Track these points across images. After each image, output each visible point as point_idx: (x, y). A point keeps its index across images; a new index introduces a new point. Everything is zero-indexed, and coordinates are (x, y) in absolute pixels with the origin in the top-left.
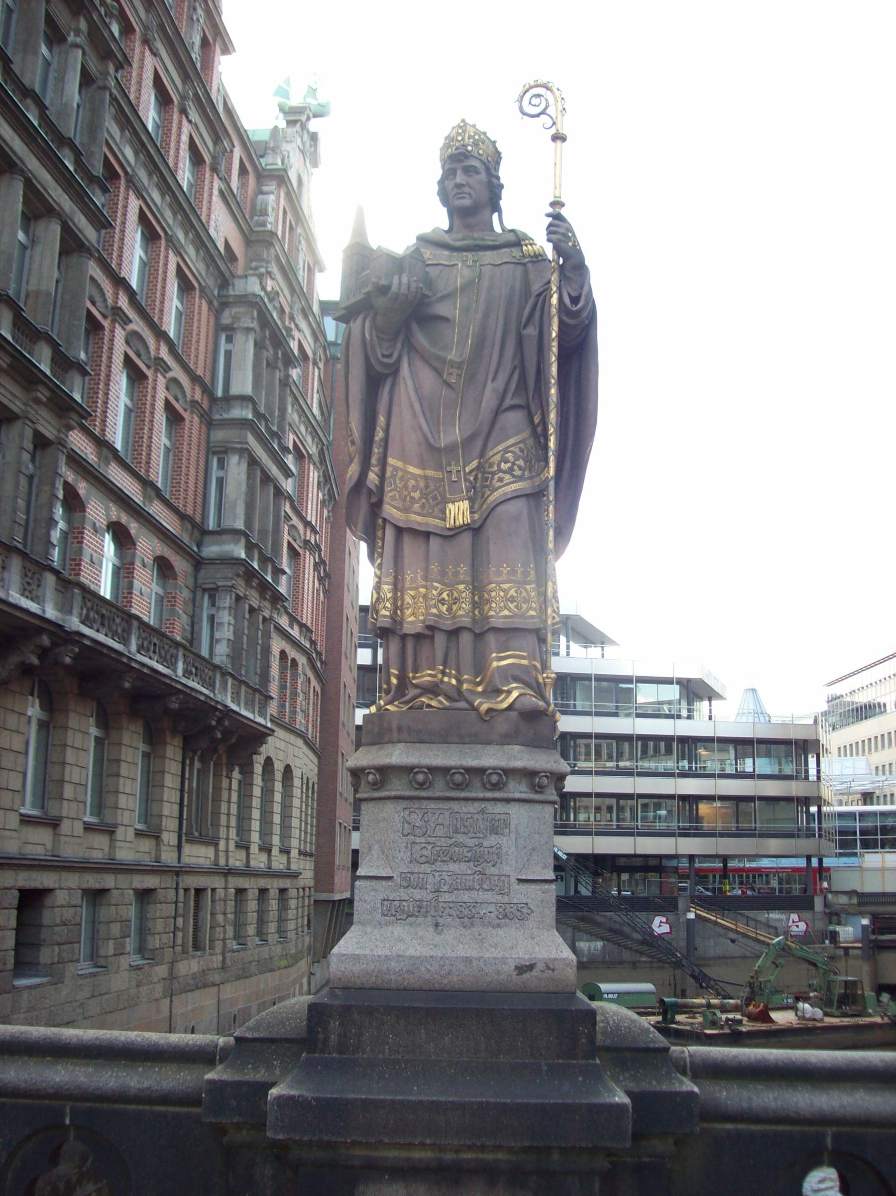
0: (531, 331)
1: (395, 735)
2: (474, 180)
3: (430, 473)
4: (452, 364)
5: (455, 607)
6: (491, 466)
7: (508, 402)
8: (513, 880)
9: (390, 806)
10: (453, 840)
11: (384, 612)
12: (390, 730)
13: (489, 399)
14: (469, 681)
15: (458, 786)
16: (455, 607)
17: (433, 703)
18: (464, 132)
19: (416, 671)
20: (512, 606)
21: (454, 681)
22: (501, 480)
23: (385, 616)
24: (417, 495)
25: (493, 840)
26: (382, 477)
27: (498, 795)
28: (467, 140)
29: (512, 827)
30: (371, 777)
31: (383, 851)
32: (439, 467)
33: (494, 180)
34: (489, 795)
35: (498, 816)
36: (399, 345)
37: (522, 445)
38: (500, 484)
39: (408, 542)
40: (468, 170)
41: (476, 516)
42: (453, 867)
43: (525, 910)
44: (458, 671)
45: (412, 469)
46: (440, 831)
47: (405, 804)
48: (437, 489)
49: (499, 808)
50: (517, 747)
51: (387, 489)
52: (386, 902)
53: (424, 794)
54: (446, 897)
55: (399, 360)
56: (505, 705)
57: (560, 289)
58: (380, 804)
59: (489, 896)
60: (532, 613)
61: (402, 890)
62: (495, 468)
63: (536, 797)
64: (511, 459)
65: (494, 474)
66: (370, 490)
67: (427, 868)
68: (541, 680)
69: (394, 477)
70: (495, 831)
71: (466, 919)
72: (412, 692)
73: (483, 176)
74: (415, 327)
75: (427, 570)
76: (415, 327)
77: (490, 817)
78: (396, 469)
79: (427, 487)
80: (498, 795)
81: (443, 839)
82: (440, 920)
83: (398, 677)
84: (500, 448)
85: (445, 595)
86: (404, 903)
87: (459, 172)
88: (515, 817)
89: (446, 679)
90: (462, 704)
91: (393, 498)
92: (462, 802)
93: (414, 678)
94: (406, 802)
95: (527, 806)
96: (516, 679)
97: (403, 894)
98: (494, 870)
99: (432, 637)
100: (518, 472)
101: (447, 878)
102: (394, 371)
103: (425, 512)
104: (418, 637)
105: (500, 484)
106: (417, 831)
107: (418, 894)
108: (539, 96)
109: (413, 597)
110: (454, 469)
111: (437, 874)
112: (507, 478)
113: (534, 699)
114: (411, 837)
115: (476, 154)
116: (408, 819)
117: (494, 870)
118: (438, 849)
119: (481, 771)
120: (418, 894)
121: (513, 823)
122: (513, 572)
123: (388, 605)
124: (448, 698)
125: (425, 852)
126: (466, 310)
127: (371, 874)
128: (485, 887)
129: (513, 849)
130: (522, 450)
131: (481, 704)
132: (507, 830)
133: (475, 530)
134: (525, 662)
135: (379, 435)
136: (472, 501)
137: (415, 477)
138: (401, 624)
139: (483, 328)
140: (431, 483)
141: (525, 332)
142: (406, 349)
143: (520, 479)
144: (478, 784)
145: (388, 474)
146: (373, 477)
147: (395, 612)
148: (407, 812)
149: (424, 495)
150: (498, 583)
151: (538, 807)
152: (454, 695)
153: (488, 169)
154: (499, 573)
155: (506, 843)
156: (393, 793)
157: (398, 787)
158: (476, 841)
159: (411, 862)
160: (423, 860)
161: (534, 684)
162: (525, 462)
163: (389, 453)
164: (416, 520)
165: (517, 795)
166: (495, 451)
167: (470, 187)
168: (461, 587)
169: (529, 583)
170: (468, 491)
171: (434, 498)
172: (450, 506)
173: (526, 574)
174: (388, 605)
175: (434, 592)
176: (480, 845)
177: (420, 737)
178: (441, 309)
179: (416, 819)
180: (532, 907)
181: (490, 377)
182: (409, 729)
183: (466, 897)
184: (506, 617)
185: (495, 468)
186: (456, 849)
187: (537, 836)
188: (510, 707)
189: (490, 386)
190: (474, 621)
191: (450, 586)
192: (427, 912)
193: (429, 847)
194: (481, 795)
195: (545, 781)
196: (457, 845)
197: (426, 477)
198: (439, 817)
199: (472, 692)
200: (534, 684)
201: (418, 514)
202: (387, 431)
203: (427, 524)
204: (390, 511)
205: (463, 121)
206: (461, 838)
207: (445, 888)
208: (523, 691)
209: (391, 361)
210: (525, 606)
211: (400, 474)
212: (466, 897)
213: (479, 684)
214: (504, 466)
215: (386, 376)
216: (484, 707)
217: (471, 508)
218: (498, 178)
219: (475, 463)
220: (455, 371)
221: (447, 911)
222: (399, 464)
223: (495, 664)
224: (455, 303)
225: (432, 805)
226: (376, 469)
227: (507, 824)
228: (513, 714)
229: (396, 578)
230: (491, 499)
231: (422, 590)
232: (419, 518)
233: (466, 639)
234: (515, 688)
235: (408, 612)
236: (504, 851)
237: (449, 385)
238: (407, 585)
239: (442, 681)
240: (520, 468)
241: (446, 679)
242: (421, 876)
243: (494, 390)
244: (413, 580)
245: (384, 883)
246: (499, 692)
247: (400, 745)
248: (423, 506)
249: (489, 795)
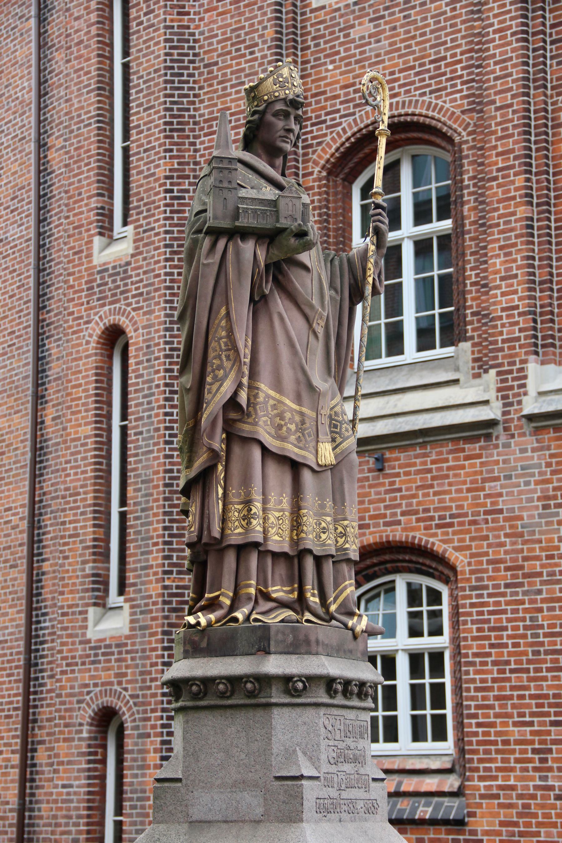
1: (314, 648)
9: (310, 712)
16: (324, 536)
24: (293, 427)
45: (288, 402)
58: (298, 710)
69: (266, 403)
78: (268, 396)
103: (301, 445)
109: (278, 518)
137: (292, 410)
140: (307, 420)
156: (309, 700)
164: (292, 450)
197: (302, 414)
203: (304, 457)
232: (296, 450)
248: (299, 439)
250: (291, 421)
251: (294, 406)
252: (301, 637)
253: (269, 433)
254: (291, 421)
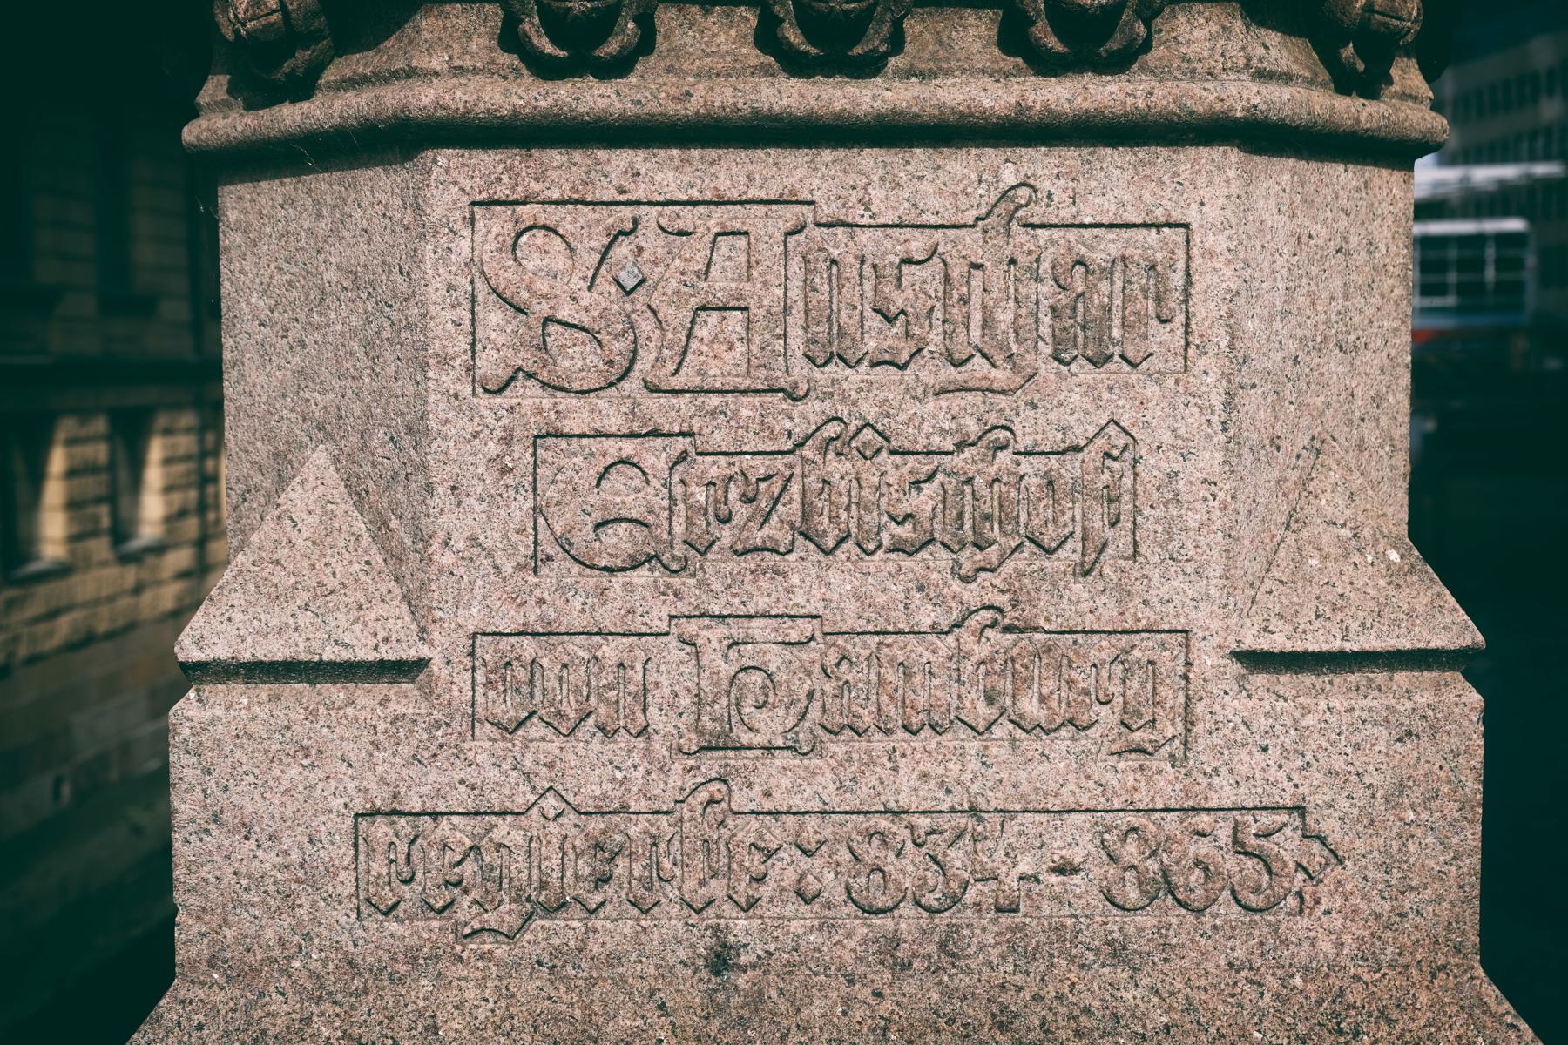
8: (1207, 660)
10: (814, 409)
25: (1072, 402)
29: (1206, 311)
31: (358, 495)
35: (1111, 245)
42: (824, 586)
43: (1288, 846)
46: (721, 354)
49: (1114, 183)
52: (380, 830)
53: (593, 97)
54: (782, 781)
59: (1054, 767)
61: (483, 745)
70: (1085, 339)
71: (908, 919)
77: (1052, 247)
81: (747, 408)
82: (740, 926)
86: (503, 830)
88: (1219, 242)
92: (869, 159)
94: (488, 160)
95: (1281, 176)
97: (488, 766)
98: (1081, 602)
101: (775, 659)
107: (593, 768)
111: (713, 636)
114: (528, 395)
116: (505, 275)
117: (1081, 602)
118: (715, 468)
120: (593, 768)
121: (1215, 279)
125: (624, 493)
127: (277, 651)
128: (1030, 706)
129: (1209, 460)
132: (1165, 337)
148: (497, 225)
155: (1169, 419)
158: (969, 413)
159: (537, 561)
160: (619, 540)
165: (1241, 96)
176: (994, 439)
180: (1330, 826)
183: (911, 776)
186: (836, 467)
187: (1334, 365)
192: (656, 878)
193: (655, 457)
206: (867, 393)
207: (770, 725)
212: (911, 776)
221: (785, 870)
225: (663, 172)
227: (1168, 295)
236: (1154, 466)
242: (610, 651)
245: (366, 696)
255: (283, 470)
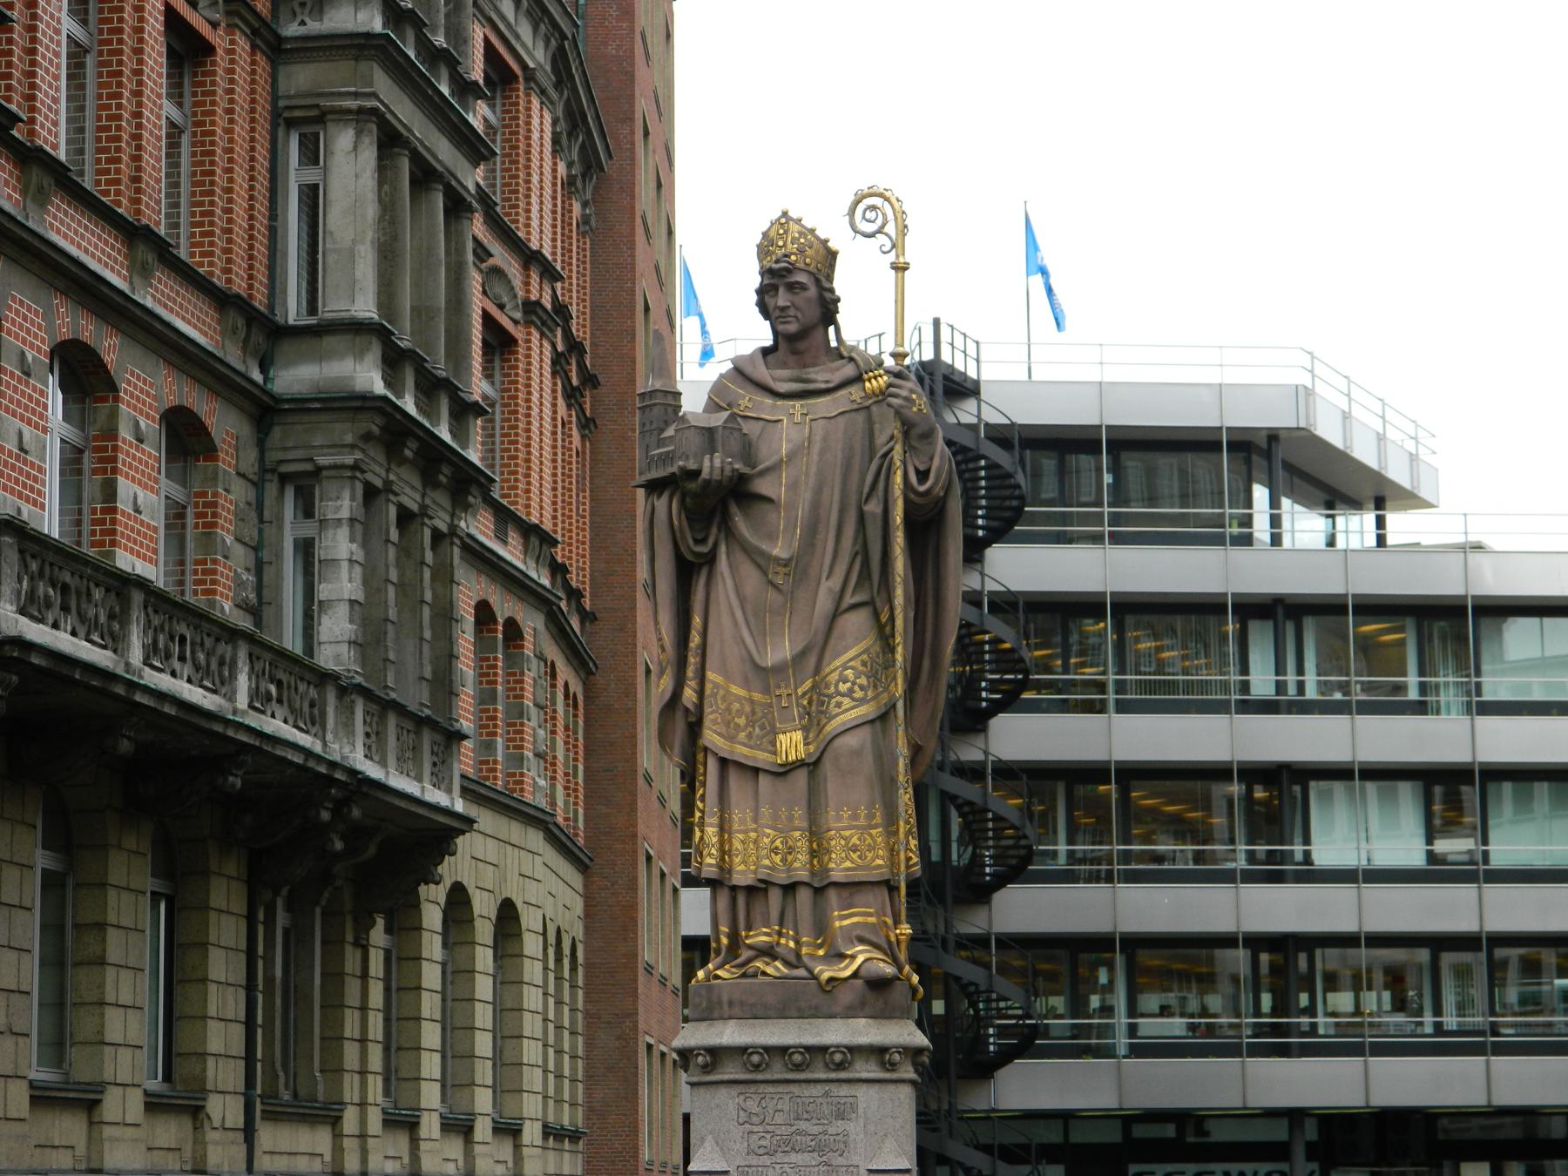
0: (874, 507)
2: (800, 298)
3: (757, 696)
4: (777, 560)
5: (790, 858)
6: (827, 686)
7: (849, 600)
9: (723, 1093)
11: (709, 860)
12: (720, 1003)
13: (824, 603)
14: (809, 944)
15: (798, 1067)
16: (790, 858)
17: (769, 970)
18: (786, 232)
19: (749, 928)
20: (854, 856)
21: (792, 944)
22: (839, 705)
23: (710, 865)
24: (742, 721)
25: (838, 1126)
26: (701, 693)
27: (843, 1075)
28: (789, 246)
29: (860, 1111)
30: (700, 1059)
32: (766, 691)
33: (827, 295)
34: (833, 1075)
36: (714, 530)
37: (865, 657)
38: (837, 710)
39: (734, 778)
40: (791, 287)
41: (812, 748)
42: (793, 1158)
44: (797, 932)
45: (735, 689)
47: (741, 1088)
48: (765, 716)
49: (844, 1090)
50: (863, 1021)
51: (707, 710)
53: (760, 1077)
55: (716, 546)
56: (848, 973)
57: (904, 463)
60: (880, 862)
62: (832, 689)
63: (888, 1076)
64: (851, 677)
65: (830, 697)
66: (687, 710)
67: (766, 1160)
68: (893, 939)
69: (714, 695)
70: (841, 1116)
72: (745, 954)
73: (813, 292)
74: (734, 508)
75: (756, 810)
76: (734, 508)
78: (716, 686)
79: (753, 713)
80: (843, 1075)
83: (729, 936)
84: (837, 663)
85: (778, 843)
87: (781, 290)
89: (783, 941)
90: (802, 972)
91: (715, 722)
93: (747, 937)
95: (876, 1087)
96: (862, 940)
98: (841, 1161)
99: (766, 891)
100: (859, 694)
102: (711, 559)
104: (750, 890)
105: (837, 710)
106: (755, 1120)
108: (873, 208)
110: (784, 692)
112: (847, 702)
113: (882, 965)
115: (801, 265)
117: (841, 1161)
119: (823, 1049)
121: (862, 1106)
122: (855, 817)
123: (713, 851)
124: (787, 963)
125: (763, 1143)
126: (793, 487)
130: (864, 664)
131: (822, 972)
133: (812, 766)
134: (872, 920)
135: (695, 640)
136: (806, 729)
137: (739, 699)
138: (730, 872)
139: (816, 506)
140: (758, 709)
141: (867, 508)
142: (722, 535)
143: (862, 701)
144: (821, 1065)
145: (708, 691)
146: (689, 695)
147: (723, 859)
149: (751, 723)
150: (838, 830)
151: (891, 1087)
152: (792, 958)
153: (818, 281)
154: (839, 818)
155: (853, 1128)
156: (726, 1077)
157: (730, 1071)
158: (820, 1129)
160: (762, 1151)
161: (885, 945)
162: (868, 678)
163: (708, 666)
164: (741, 752)
165: (864, 1075)
166: (832, 667)
167: (797, 309)
168: (797, 834)
169: (876, 827)
170: (801, 718)
171: (762, 727)
172: (781, 736)
173: (870, 816)
174: (713, 851)
175: (766, 840)
176: (825, 1133)
177: (755, 1012)
178: (763, 486)
179: (752, 1105)
181: (824, 575)
182: (742, 1004)
184: (848, 869)
185: (832, 689)
188: (855, 975)
189: (825, 586)
190: (813, 874)
191: (784, 832)
194: (823, 1076)
195: (897, 1057)
196: (799, 1133)
197: (752, 702)
198: (779, 1104)
199: (812, 956)
200: (885, 945)
201: (745, 745)
202: (704, 634)
203: (755, 759)
204: (711, 737)
205: (785, 214)
208: (868, 955)
209: (704, 549)
210: (870, 855)
211: (722, 692)
213: (820, 946)
214: (843, 687)
215: (700, 566)
216: (826, 976)
217: (805, 738)
218: (832, 291)
219: (808, 684)
220: (782, 570)
222: (719, 679)
223: (837, 924)
224: (780, 477)
225: (770, 1089)
226: (693, 684)
228: (859, 982)
229: (722, 819)
230: (828, 728)
231: (753, 835)
232: (745, 750)
233: (804, 896)
234: (861, 952)
235: (737, 860)
236: (852, 1137)
237: (775, 586)
238: (736, 827)
239: (778, 944)
240: (862, 688)
241: (783, 941)
243: (830, 590)
244: (742, 821)
246: (842, 956)
247: (732, 1022)
248: (750, 736)
249: (833, 1075)
250: (740, 713)
251: (742, 693)
252: (715, 999)
253: (719, 734)
254: (740, 713)
255: (703, 1140)
